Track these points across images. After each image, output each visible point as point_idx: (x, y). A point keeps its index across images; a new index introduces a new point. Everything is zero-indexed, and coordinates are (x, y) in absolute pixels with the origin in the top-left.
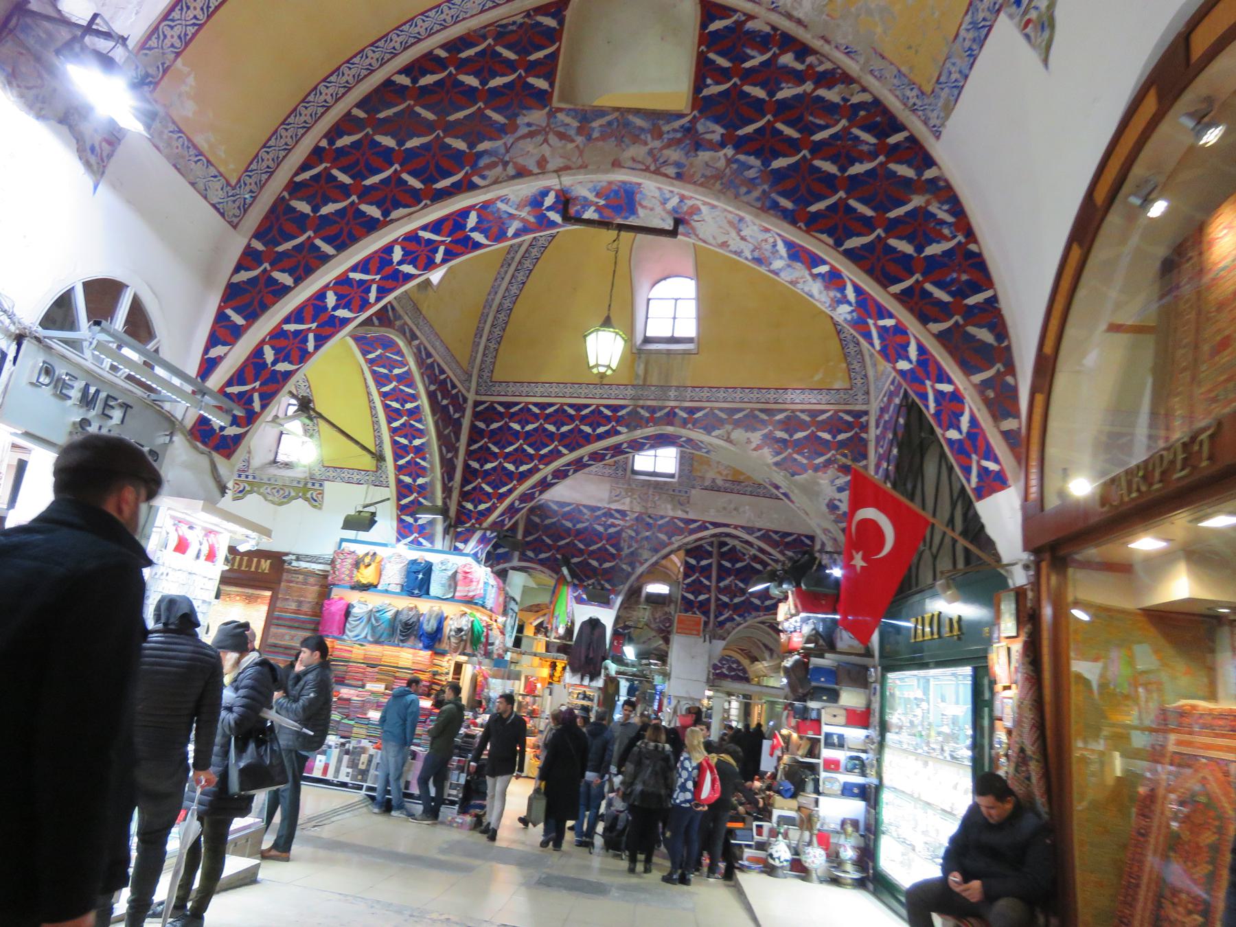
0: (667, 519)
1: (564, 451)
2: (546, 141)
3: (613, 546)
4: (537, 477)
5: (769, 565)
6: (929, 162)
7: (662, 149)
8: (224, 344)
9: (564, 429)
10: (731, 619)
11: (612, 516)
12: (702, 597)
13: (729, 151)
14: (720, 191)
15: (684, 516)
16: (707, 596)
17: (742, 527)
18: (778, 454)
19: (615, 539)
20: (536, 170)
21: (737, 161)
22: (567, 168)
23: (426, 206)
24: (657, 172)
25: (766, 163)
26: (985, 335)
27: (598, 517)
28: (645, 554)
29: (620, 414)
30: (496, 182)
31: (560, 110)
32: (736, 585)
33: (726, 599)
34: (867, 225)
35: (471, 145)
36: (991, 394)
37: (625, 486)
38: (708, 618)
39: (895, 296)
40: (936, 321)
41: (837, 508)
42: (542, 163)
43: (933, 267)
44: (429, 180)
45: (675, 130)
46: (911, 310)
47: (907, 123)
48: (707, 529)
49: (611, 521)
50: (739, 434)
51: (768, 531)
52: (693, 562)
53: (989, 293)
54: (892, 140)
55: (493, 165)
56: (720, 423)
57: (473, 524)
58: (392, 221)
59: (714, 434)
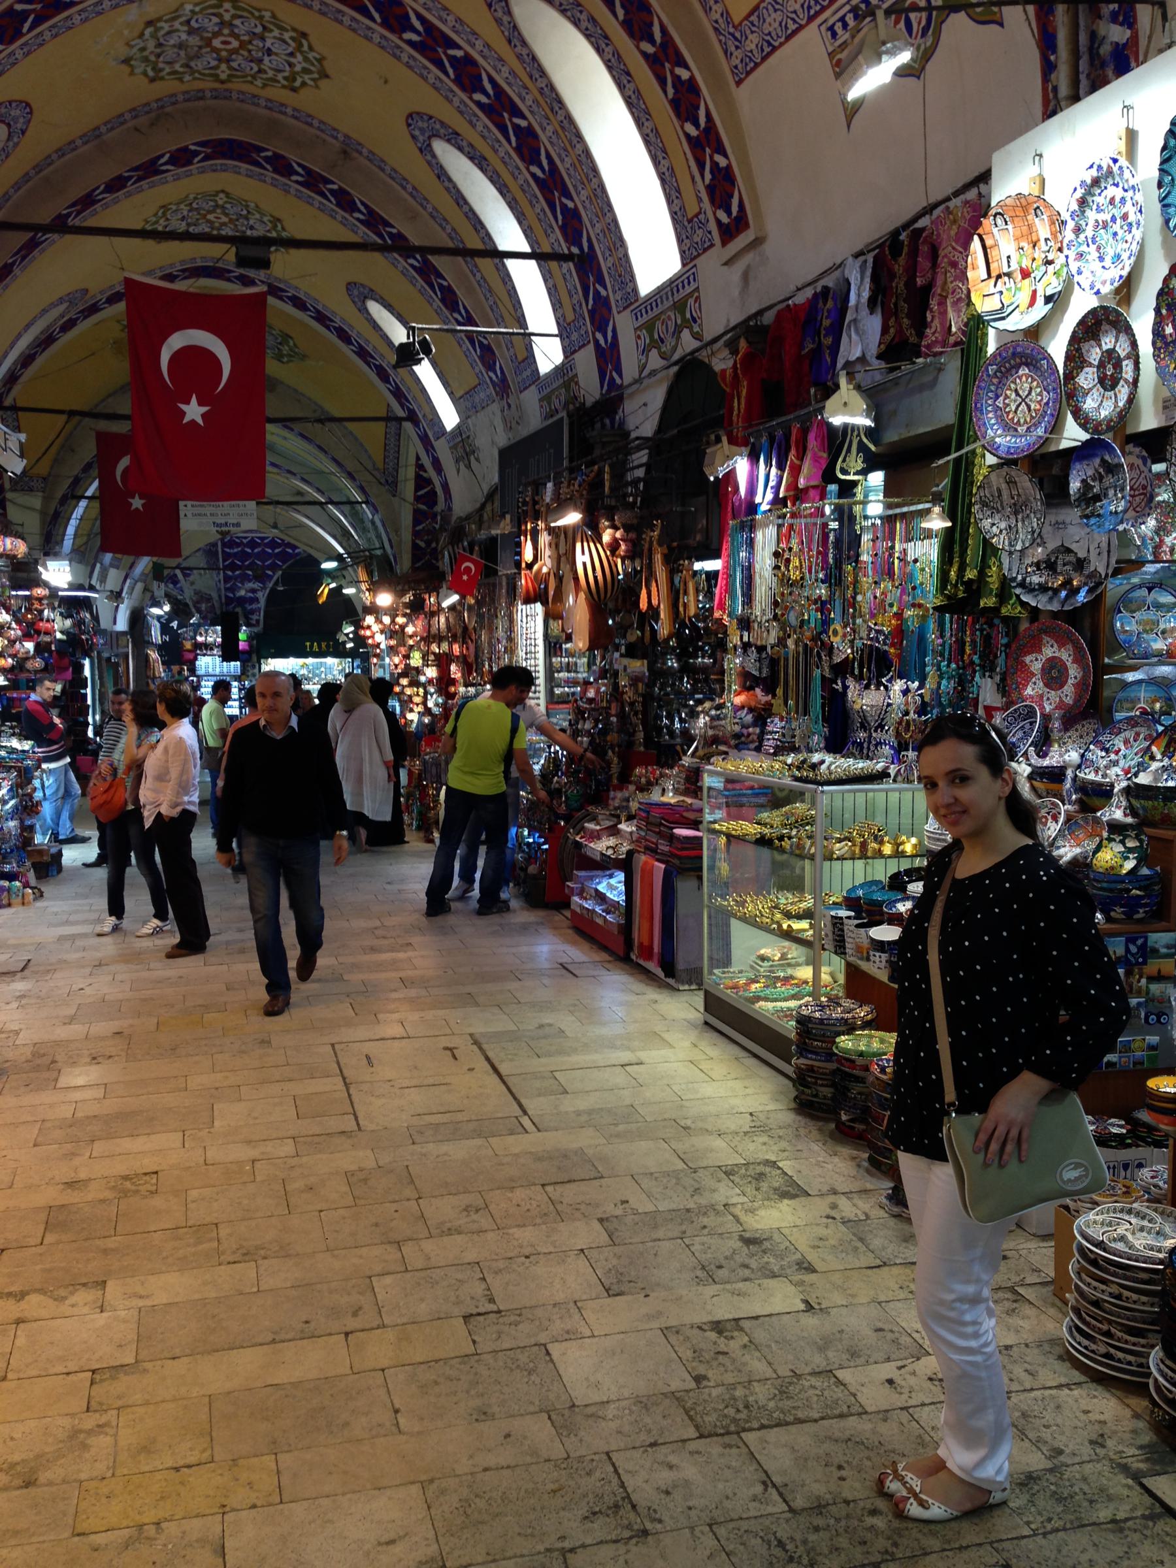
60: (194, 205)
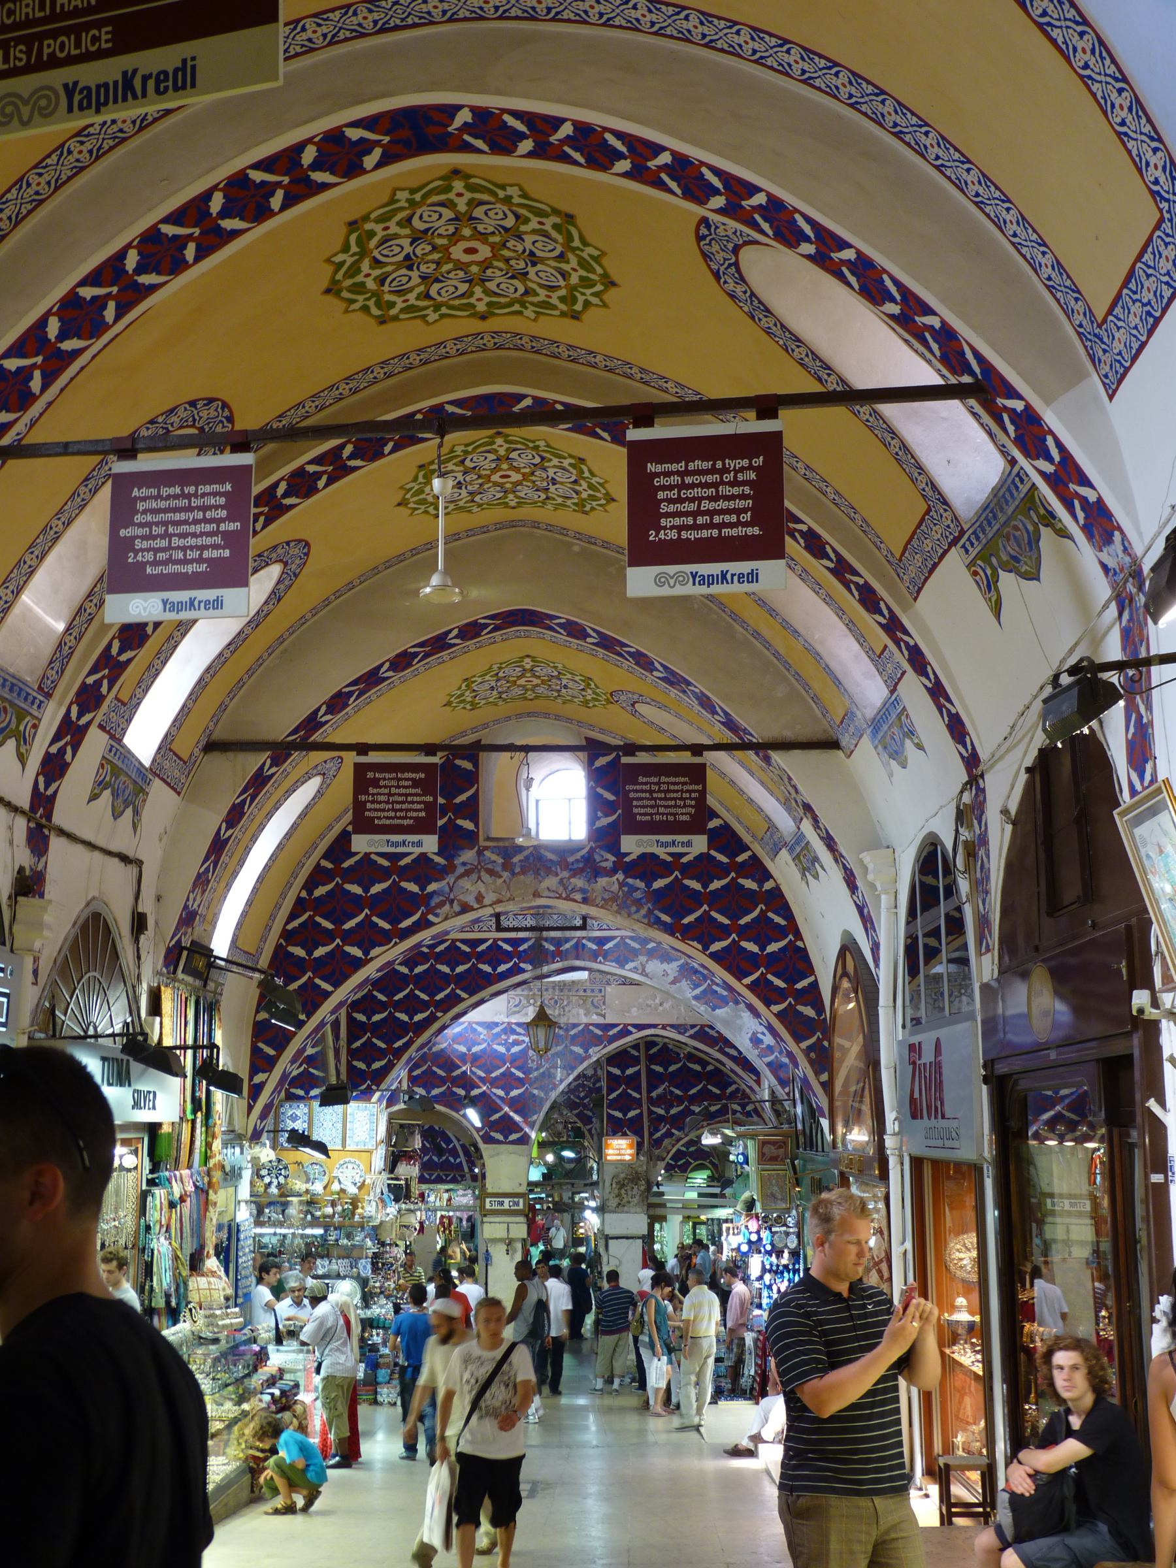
0: (580, 1028)
1: (464, 995)
2: (479, 878)
3: (518, 1068)
4: (436, 1026)
5: (709, 1063)
6: (766, 875)
7: (569, 878)
8: (264, 1072)
9: (460, 969)
10: (669, 1134)
11: (514, 1032)
12: (631, 1114)
13: (620, 876)
14: (619, 912)
15: (600, 1020)
16: (638, 1111)
17: (672, 1026)
18: (696, 986)
19: (519, 1060)
20: (476, 906)
21: (627, 884)
22: (499, 901)
23: (396, 944)
24: (568, 898)
25: (648, 885)
26: (809, 1011)
27: (498, 1035)
28: (559, 1074)
29: (521, 948)
30: (446, 919)
31: (486, 848)
32: (671, 1093)
33: (661, 1111)
34: (724, 931)
35: (423, 888)
36: (813, 1055)
37: (525, 993)
38: (642, 1137)
39: (747, 986)
40: (775, 1004)
41: (761, 1041)
42: (480, 898)
43: (772, 961)
44: (394, 922)
45: (577, 861)
46: (758, 997)
47: (751, 846)
48: (631, 1033)
49: (513, 1038)
50: (654, 966)
51: (702, 1026)
52: (617, 1071)
53: (812, 979)
54: (740, 859)
55: (441, 905)
56: (635, 954)
57: (369, 1087)
58: (372, 959)
59: (628, 967)
60: (501, 674)
